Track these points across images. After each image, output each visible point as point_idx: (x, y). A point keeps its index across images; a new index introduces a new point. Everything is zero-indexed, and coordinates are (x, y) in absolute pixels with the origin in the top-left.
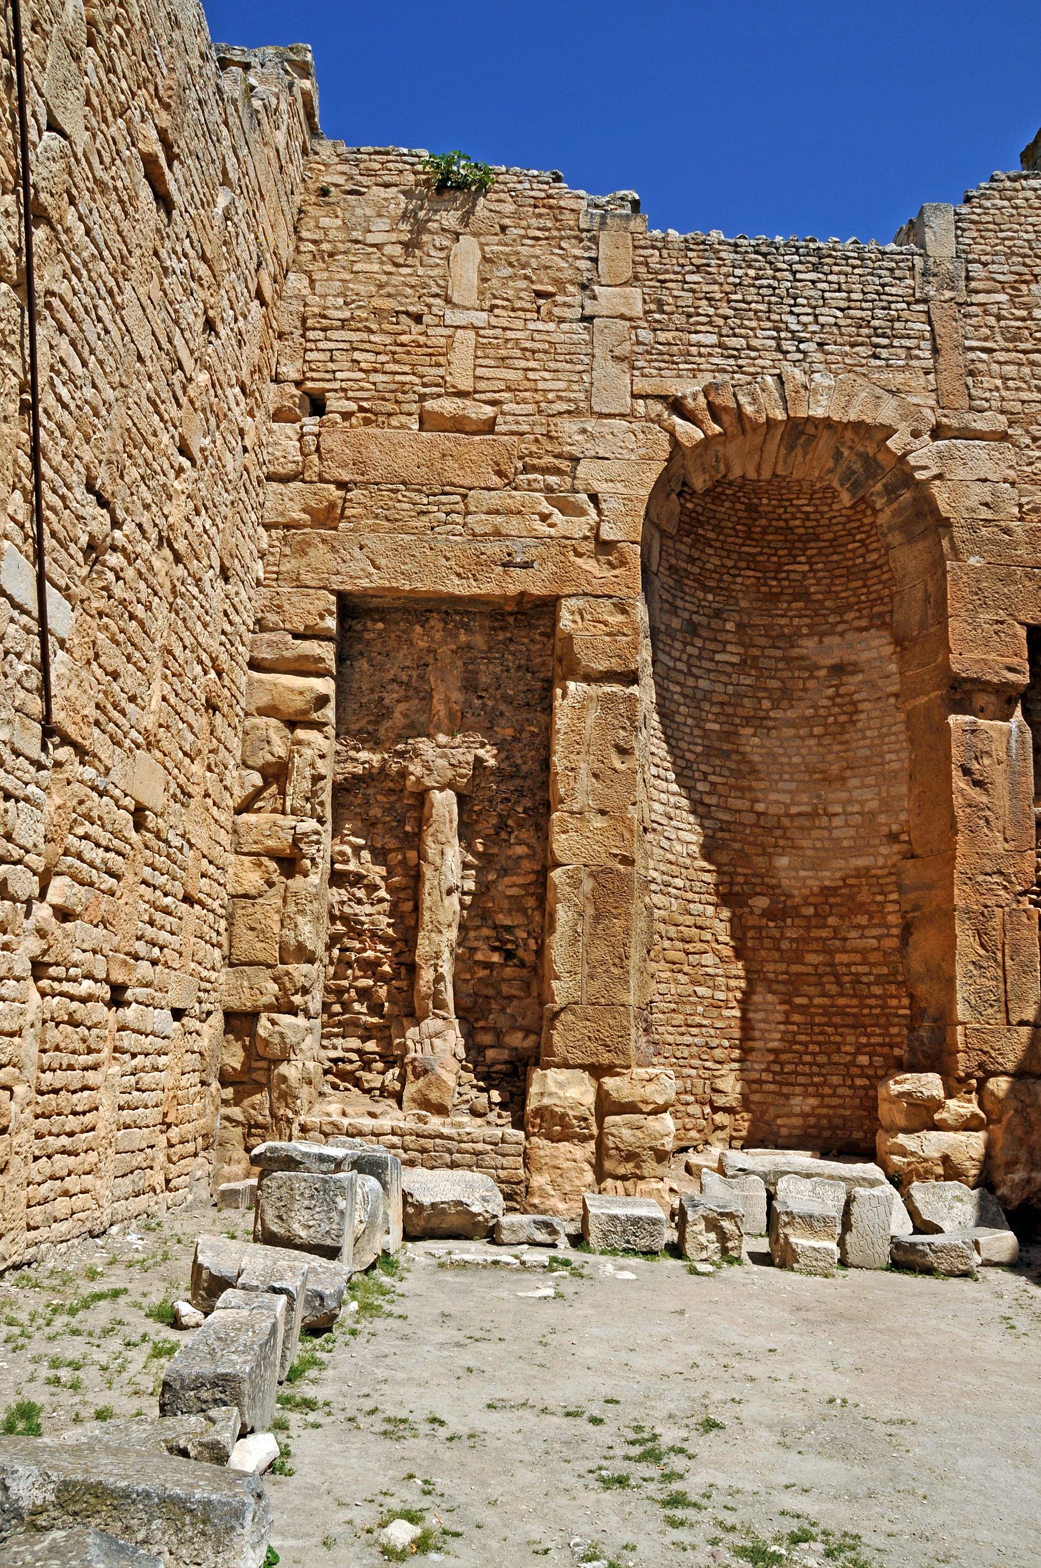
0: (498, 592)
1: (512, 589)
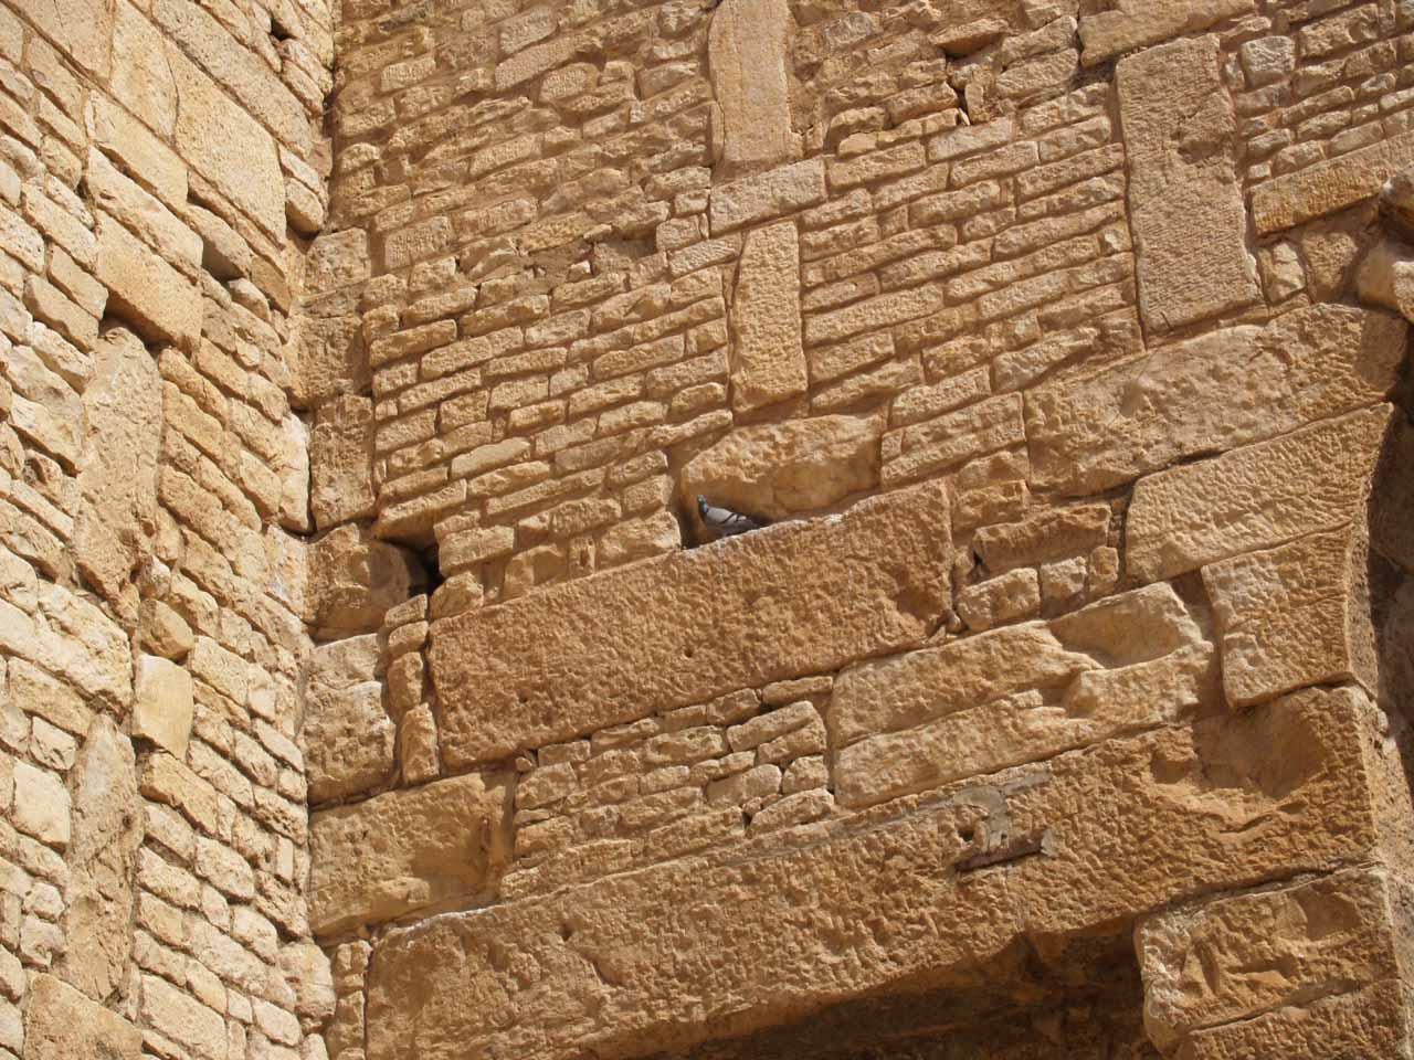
0: (949, 956)
1: (989, 938)
